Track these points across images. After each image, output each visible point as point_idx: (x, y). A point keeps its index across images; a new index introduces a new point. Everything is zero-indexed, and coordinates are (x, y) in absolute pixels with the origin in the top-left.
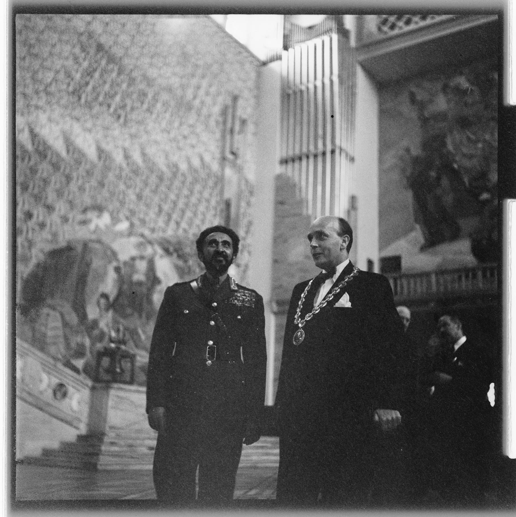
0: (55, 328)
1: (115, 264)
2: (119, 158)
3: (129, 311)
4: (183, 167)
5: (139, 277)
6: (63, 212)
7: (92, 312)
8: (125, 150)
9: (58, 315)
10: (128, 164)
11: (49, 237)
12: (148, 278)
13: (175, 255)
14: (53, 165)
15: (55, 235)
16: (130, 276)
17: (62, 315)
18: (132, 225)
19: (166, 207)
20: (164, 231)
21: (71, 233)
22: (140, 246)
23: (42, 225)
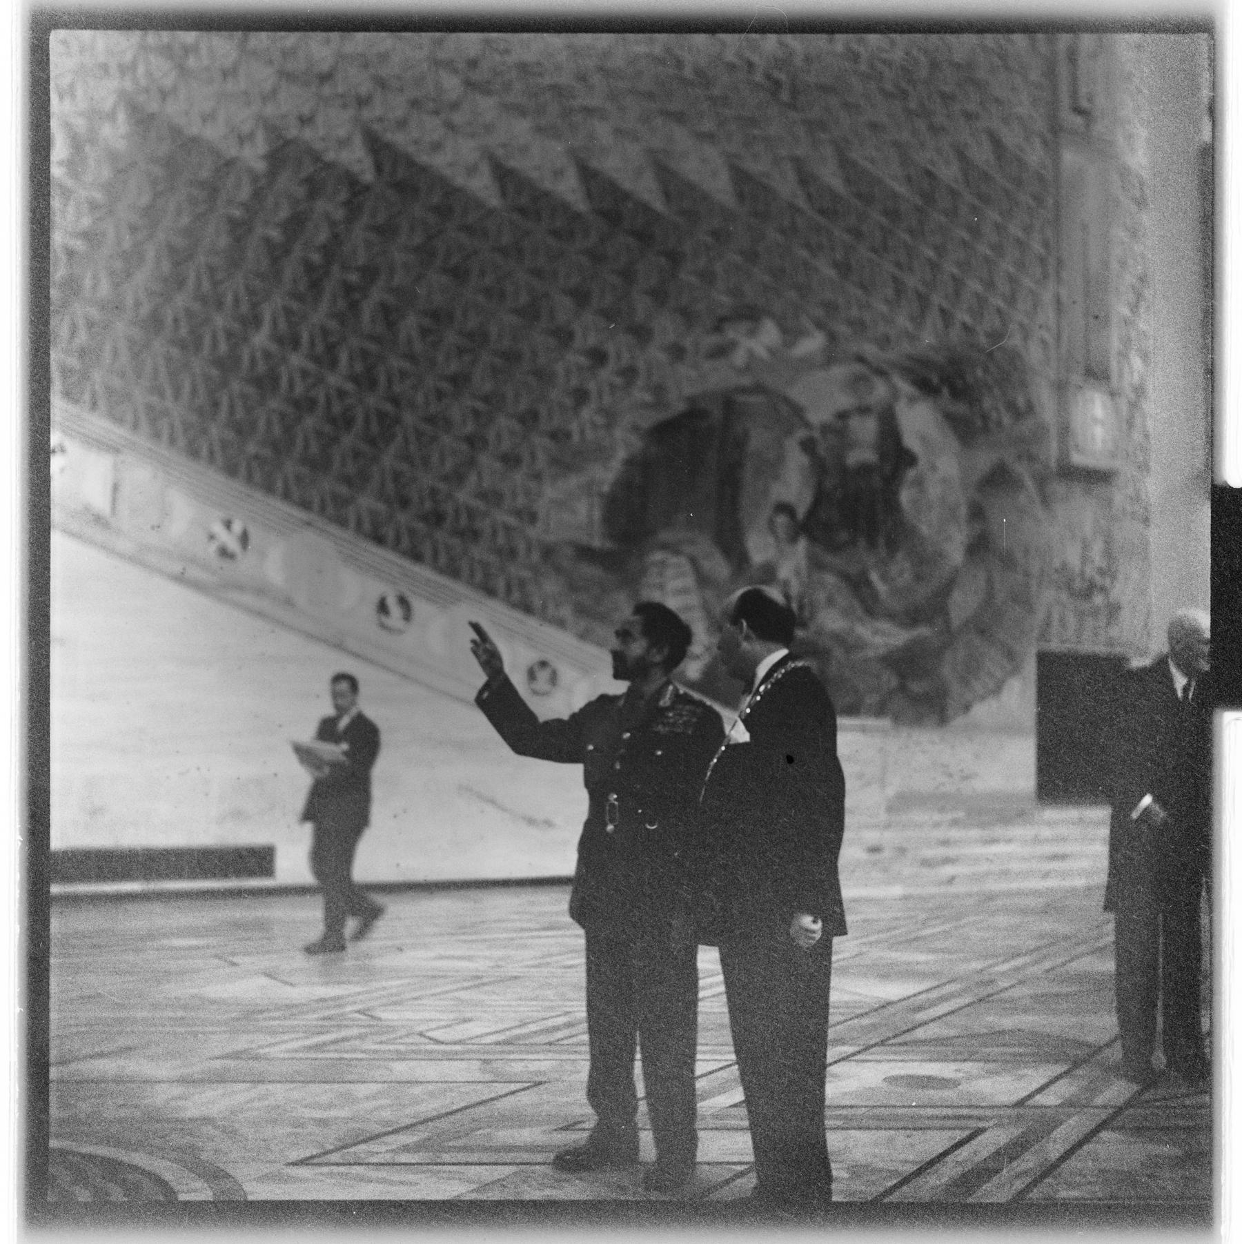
0: (683, 591)
1: (801, 434)
2: (786, 186)
3: (843, 536)
4: (949, 172)
5: (862, 455)
6: (671, 337)
8: (798, 164)
9: (683, 560)
10: (809, 197)
11: (648, 398)
12: (883, 456)
13: (945, 391)
15: (659, 390)
17: (693, 561)
18: (832, 337)
19: (912, 281)
20: (912, 338)
21: (691, 382)
22: (856, 382)
23: (629, 373)
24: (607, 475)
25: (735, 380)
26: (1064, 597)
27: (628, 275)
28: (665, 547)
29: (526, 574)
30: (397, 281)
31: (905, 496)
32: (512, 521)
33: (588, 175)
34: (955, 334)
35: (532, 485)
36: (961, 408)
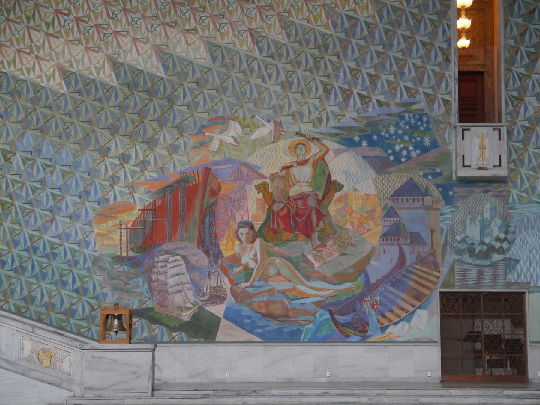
3: (286, 235)
7: (228, 247)
14: (148, 92)
16: (286, 191)
18: (278, 125)
21: (182, 163)
23: (144, 164)
24: (130, 218)
25: (213, 158)
26: (466, 258)
27: (142, 114)
28: (167, 252)
29: (85, 273)
30: (11, 137)
31: (333, 209)
32: (76, 247)
33: (116, 66)
34: (372, 111)
35: (87, 227)
36: (378, 152)
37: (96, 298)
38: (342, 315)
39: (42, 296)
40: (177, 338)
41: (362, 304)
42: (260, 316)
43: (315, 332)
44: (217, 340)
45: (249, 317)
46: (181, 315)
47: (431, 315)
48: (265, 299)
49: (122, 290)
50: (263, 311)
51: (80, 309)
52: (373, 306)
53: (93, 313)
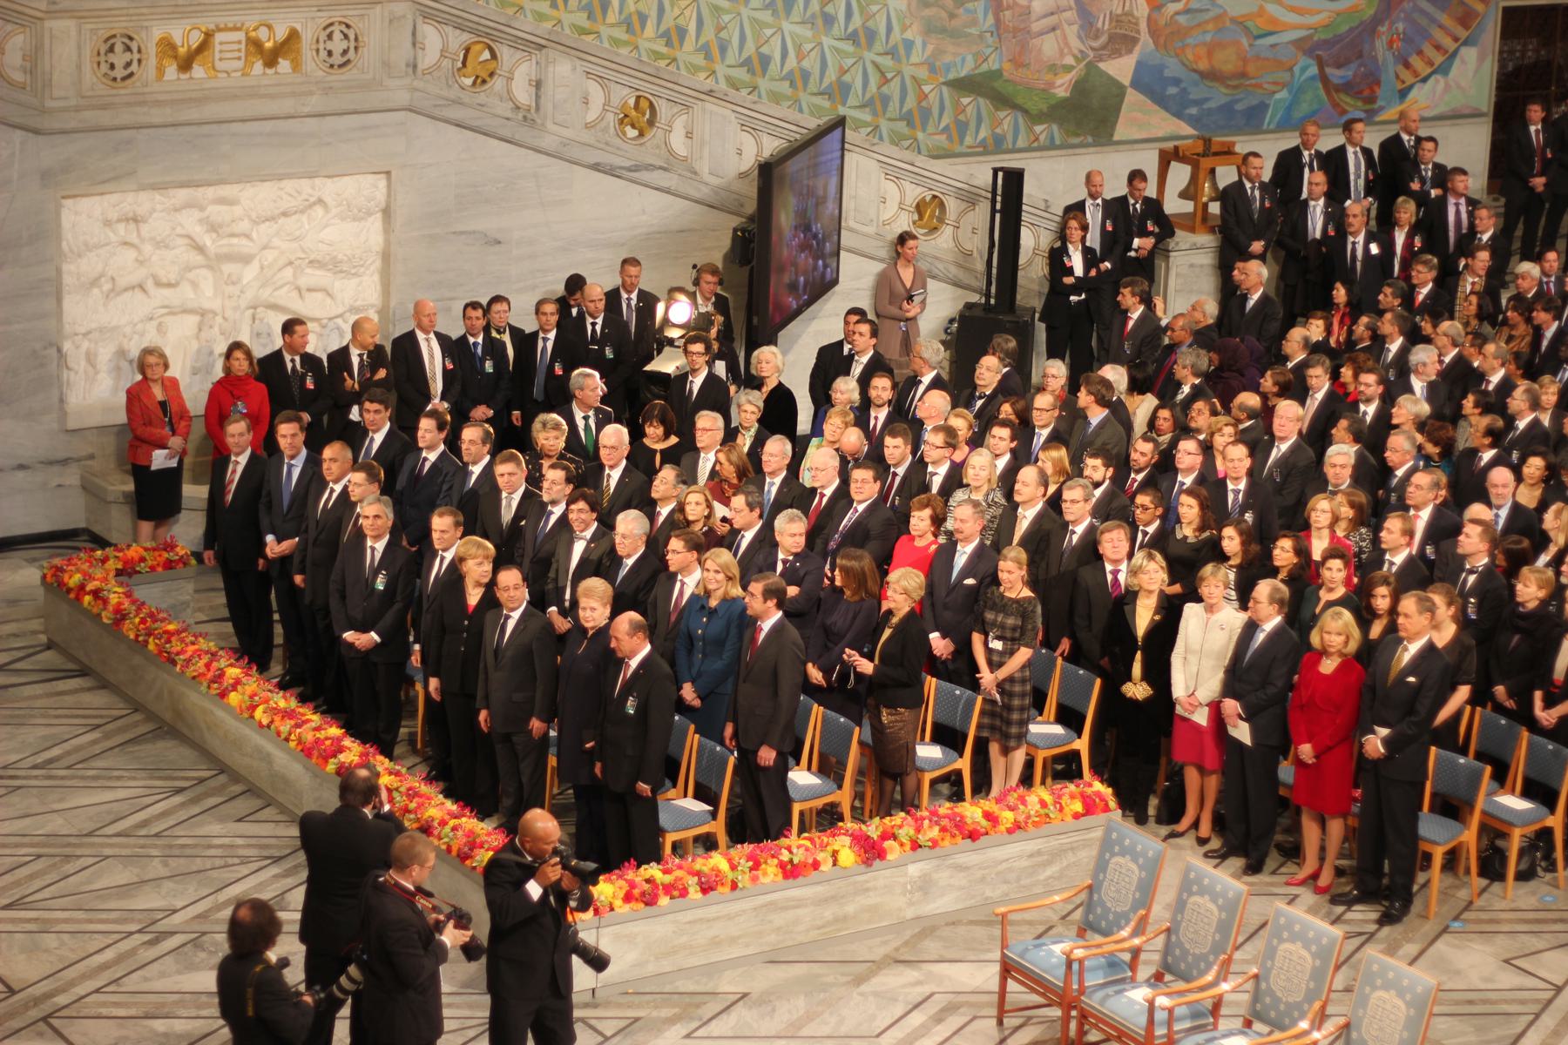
37: (892, 53)
38: (1339, 66)
39: (784, 55)
40: (1042, 138)
41: (1372, 43)
42: (1196, 77)
43: (1289, 109)
44: (1116, 137)
45: (1176, 81)
46: (1051, 85)
47: (1481, 59)
48: (1208, 38)
49: (943, 31)
50: (1203, 65)
51: (858, 84)
52: (1390, 43)
53: (885, 89)
